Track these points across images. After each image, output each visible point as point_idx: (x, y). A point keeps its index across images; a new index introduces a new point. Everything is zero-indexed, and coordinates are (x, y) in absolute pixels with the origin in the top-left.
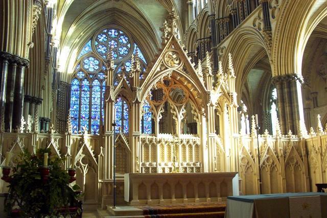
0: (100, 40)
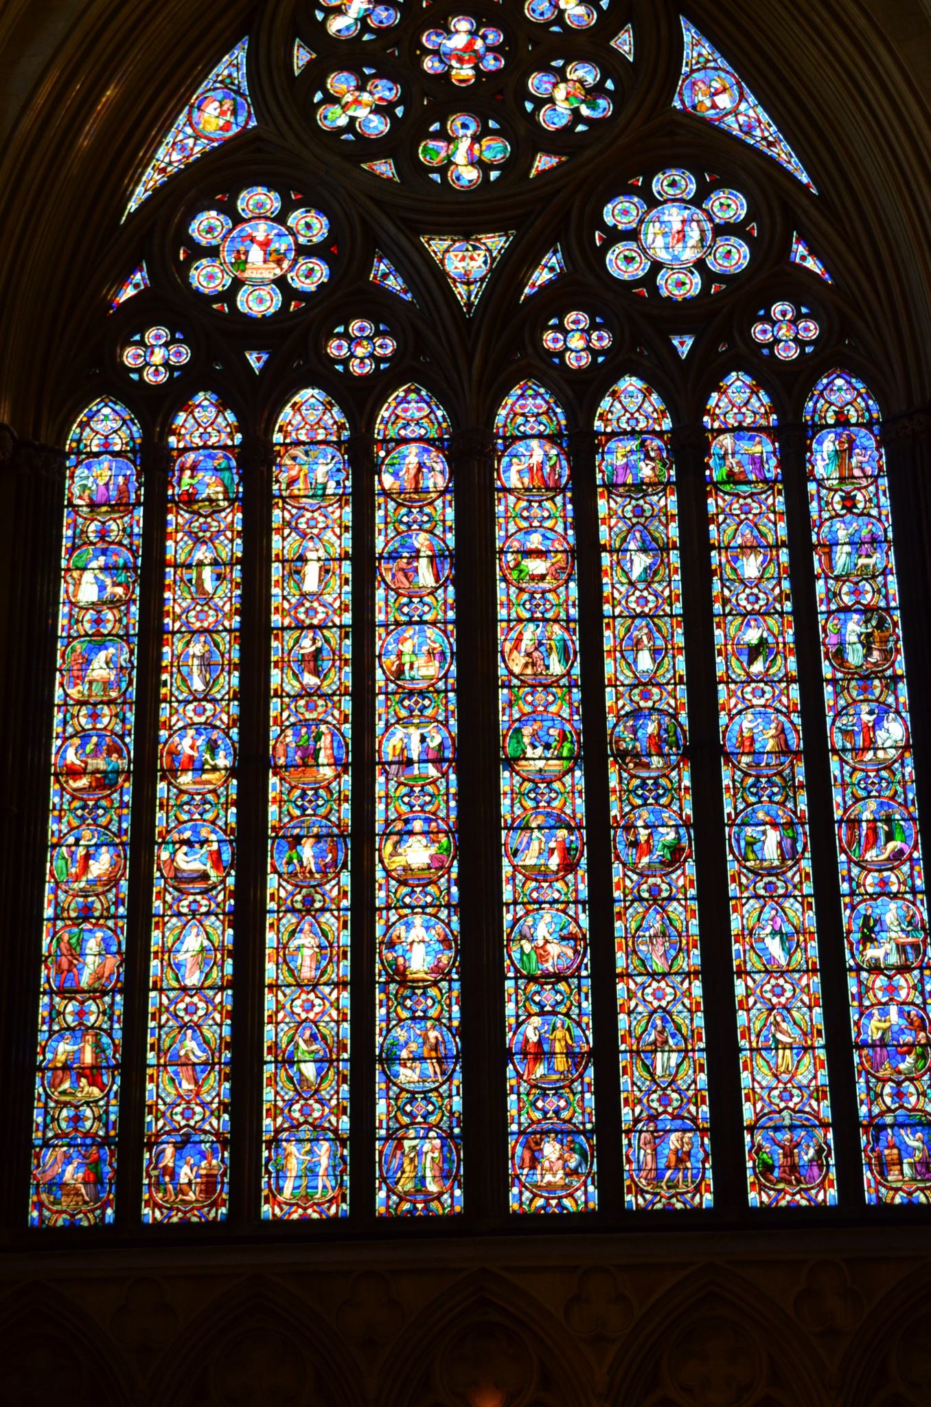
0: (336, 25)
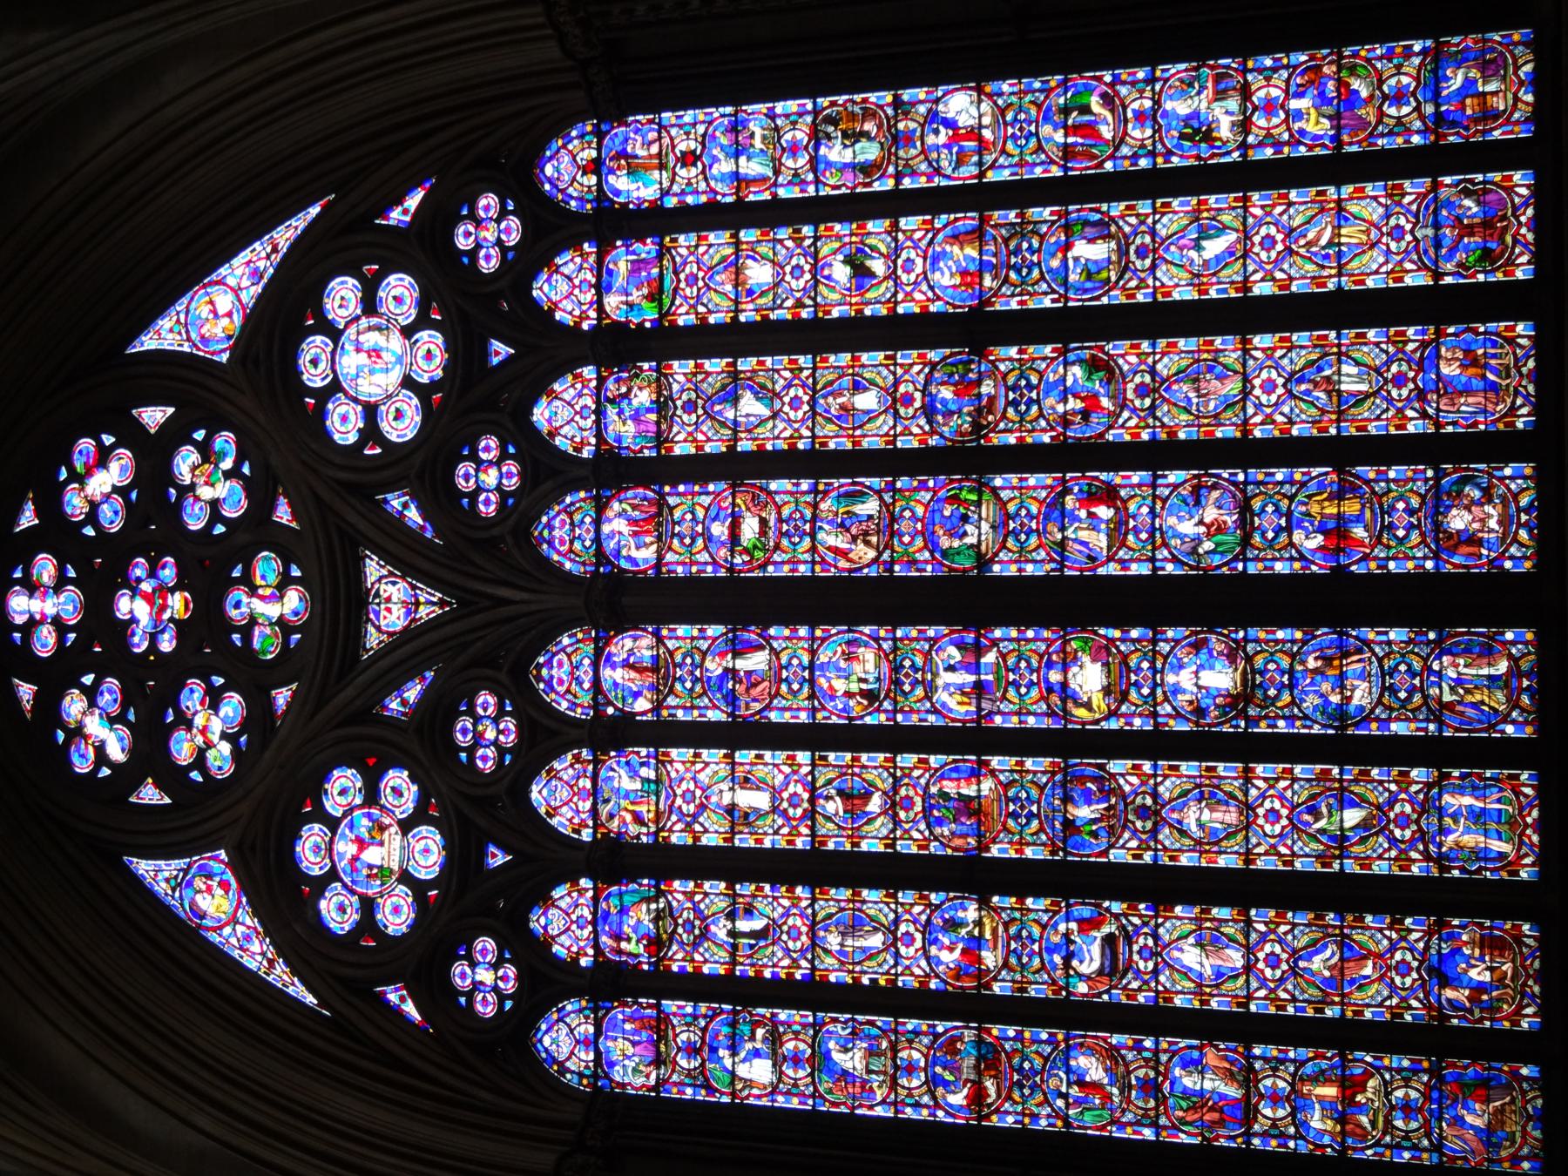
0: (116, 753)
